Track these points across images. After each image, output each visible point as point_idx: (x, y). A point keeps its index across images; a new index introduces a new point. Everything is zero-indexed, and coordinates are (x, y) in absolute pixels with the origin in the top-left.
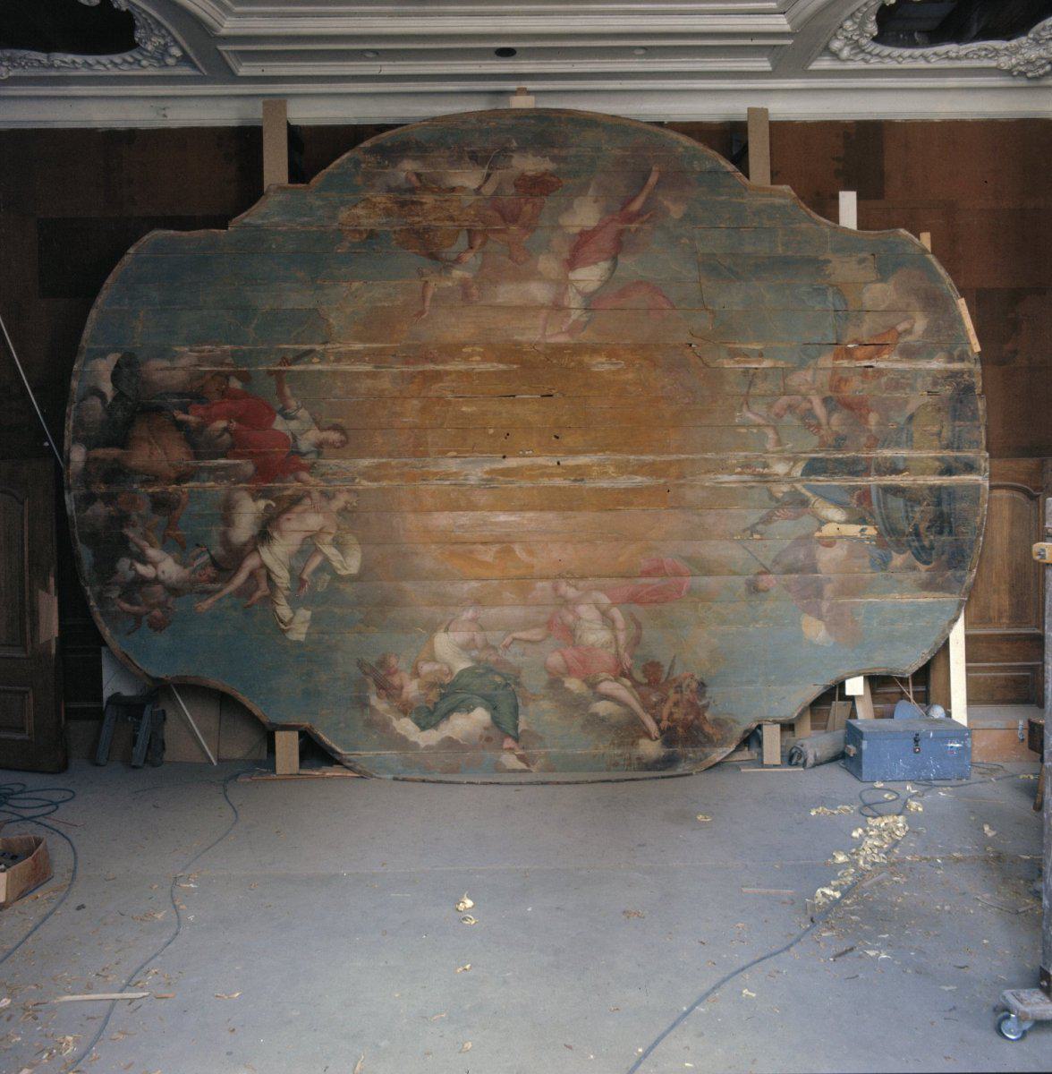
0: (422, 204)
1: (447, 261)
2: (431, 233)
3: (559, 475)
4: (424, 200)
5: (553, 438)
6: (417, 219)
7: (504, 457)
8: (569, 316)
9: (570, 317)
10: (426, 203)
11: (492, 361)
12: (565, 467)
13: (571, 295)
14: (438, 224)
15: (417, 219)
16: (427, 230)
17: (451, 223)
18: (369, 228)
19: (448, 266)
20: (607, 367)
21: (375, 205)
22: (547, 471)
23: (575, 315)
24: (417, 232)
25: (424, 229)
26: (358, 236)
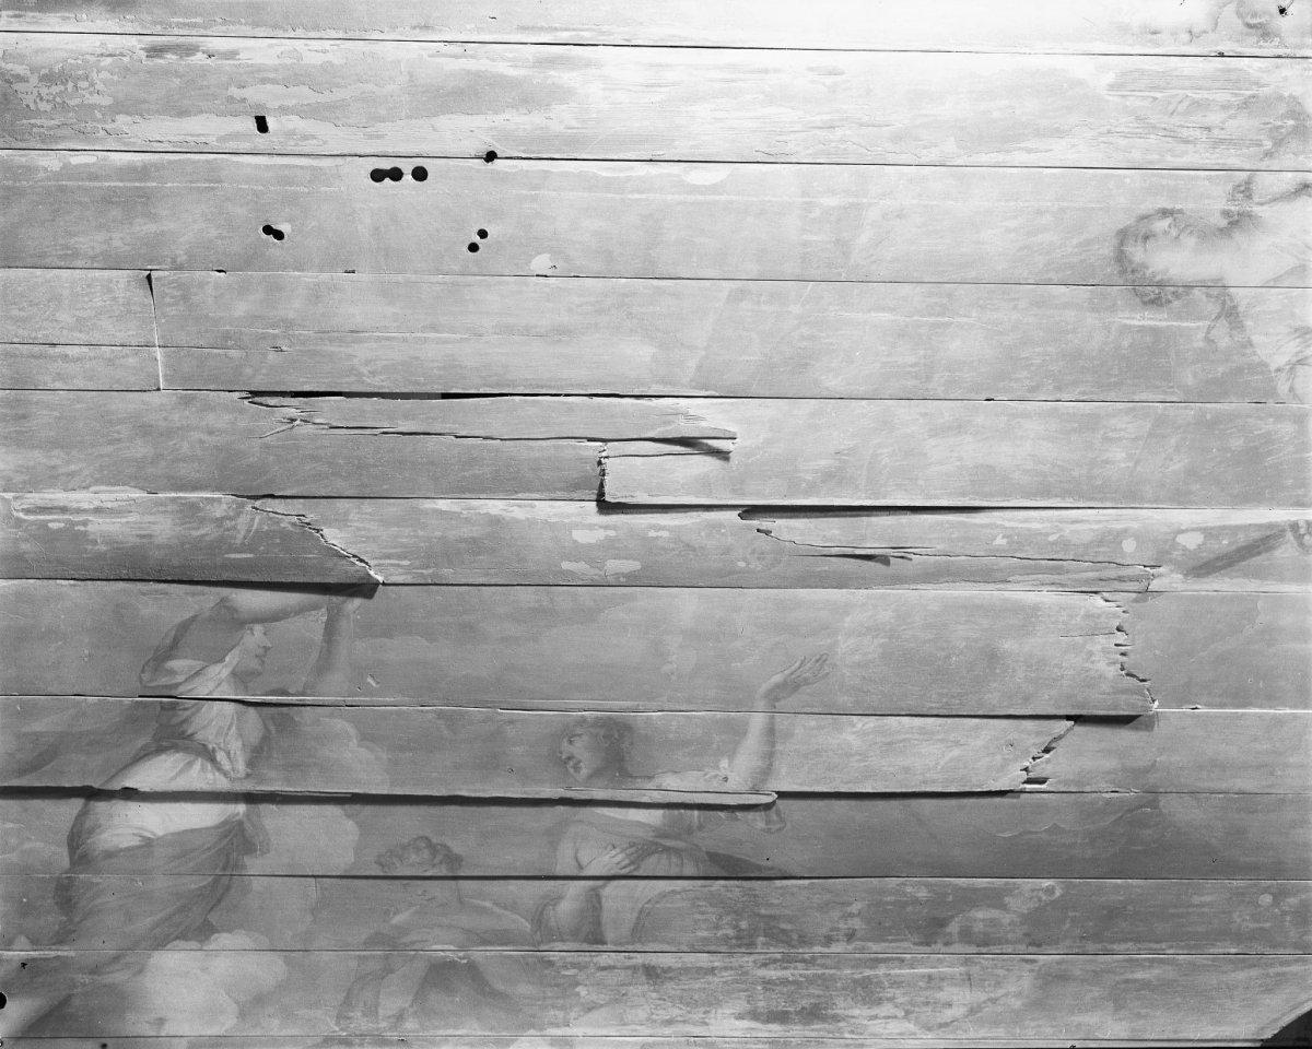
0: (754, 1015)
1: (677, 852)
2: (731, 932)
3: (260, 75)
4: (746, 1024)
5: (283, 227)
6: (773, 973)
7: (491, 156)
8: (240, 677)
9: (234, 674)
10: (740, 1017)
11: (531, 523)
12: (232, 107)
13: (235, 746)
14: (703, 960)
15: (773, 973)
16: (745, 941)
17: (653, 959)
18: (939, 947)
19: (677, 837)
20: (83, 499)
21: (907, 1013)
22: (304, 94)
23: (216, 680)
24: (776, 935)
25: (752, 944)
26: (978, 927)
